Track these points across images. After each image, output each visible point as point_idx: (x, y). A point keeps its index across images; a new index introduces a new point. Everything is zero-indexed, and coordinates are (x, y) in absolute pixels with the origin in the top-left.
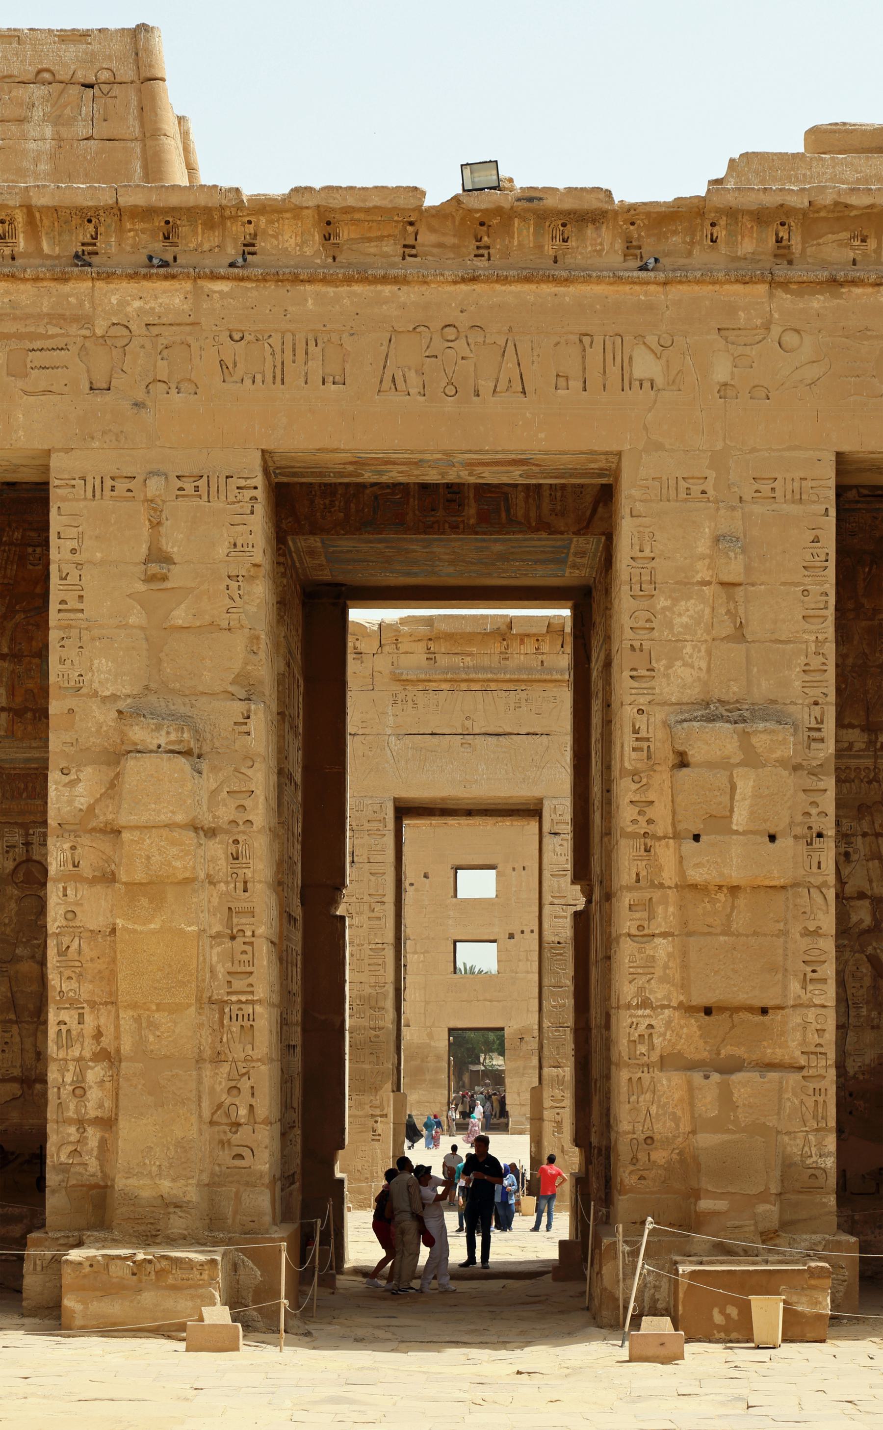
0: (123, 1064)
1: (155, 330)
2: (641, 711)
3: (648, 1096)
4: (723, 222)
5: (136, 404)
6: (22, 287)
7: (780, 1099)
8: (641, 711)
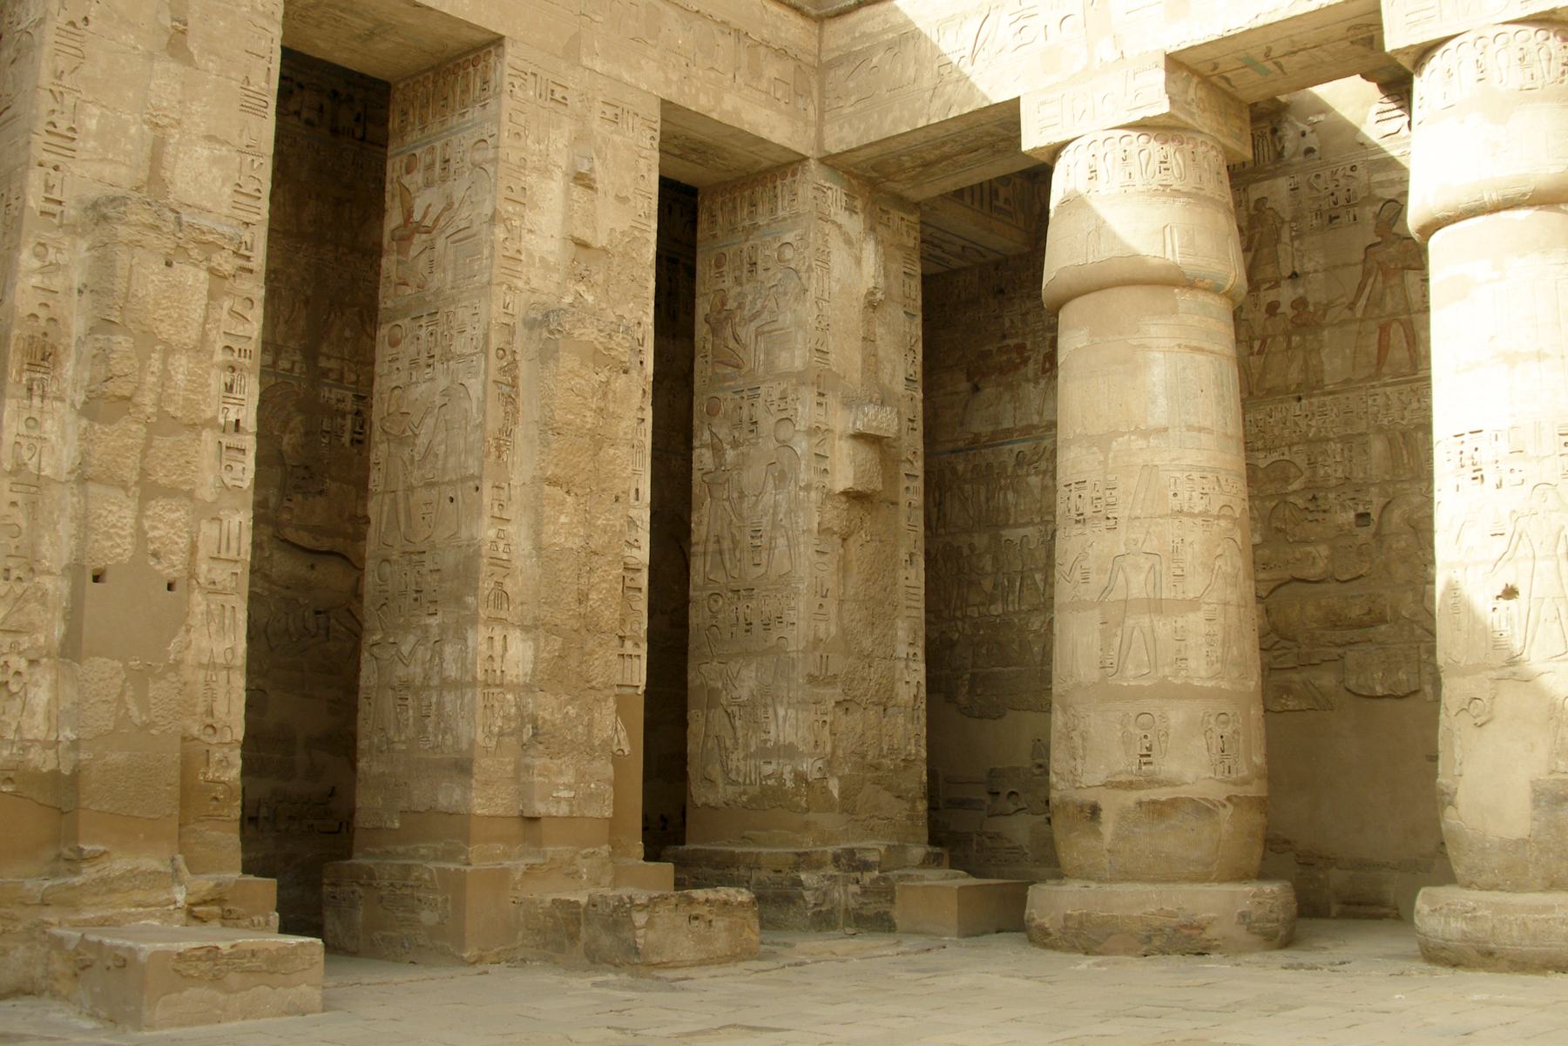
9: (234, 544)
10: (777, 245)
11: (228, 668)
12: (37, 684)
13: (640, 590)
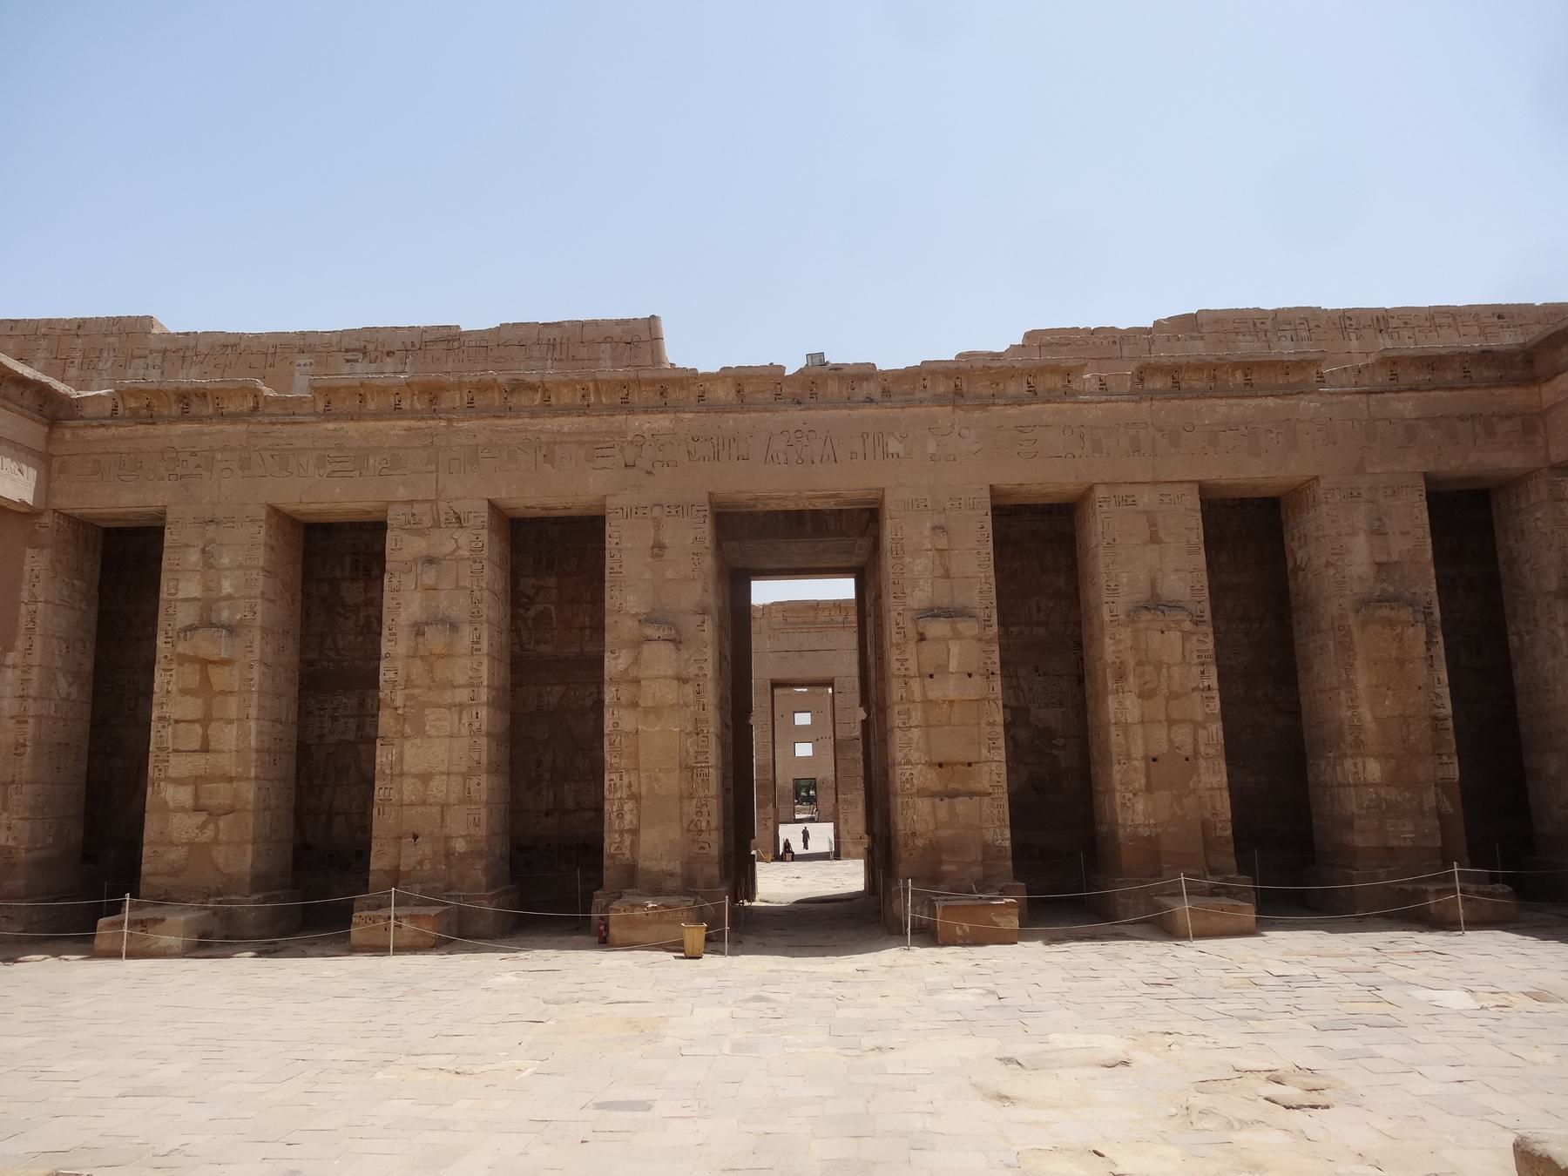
0: (643, 801)
1: (656, 437)
2: (899, 614)
3: (912, 810)
4: (929, 378)
5: (648, 472)
6: (592, 419)
7: (980, 810)
8: (899, 614)
9: (1215, 737)
10: (1533, 519)
11: (1220, 789)
12: (1138, 802)
13: (1448, 729)
